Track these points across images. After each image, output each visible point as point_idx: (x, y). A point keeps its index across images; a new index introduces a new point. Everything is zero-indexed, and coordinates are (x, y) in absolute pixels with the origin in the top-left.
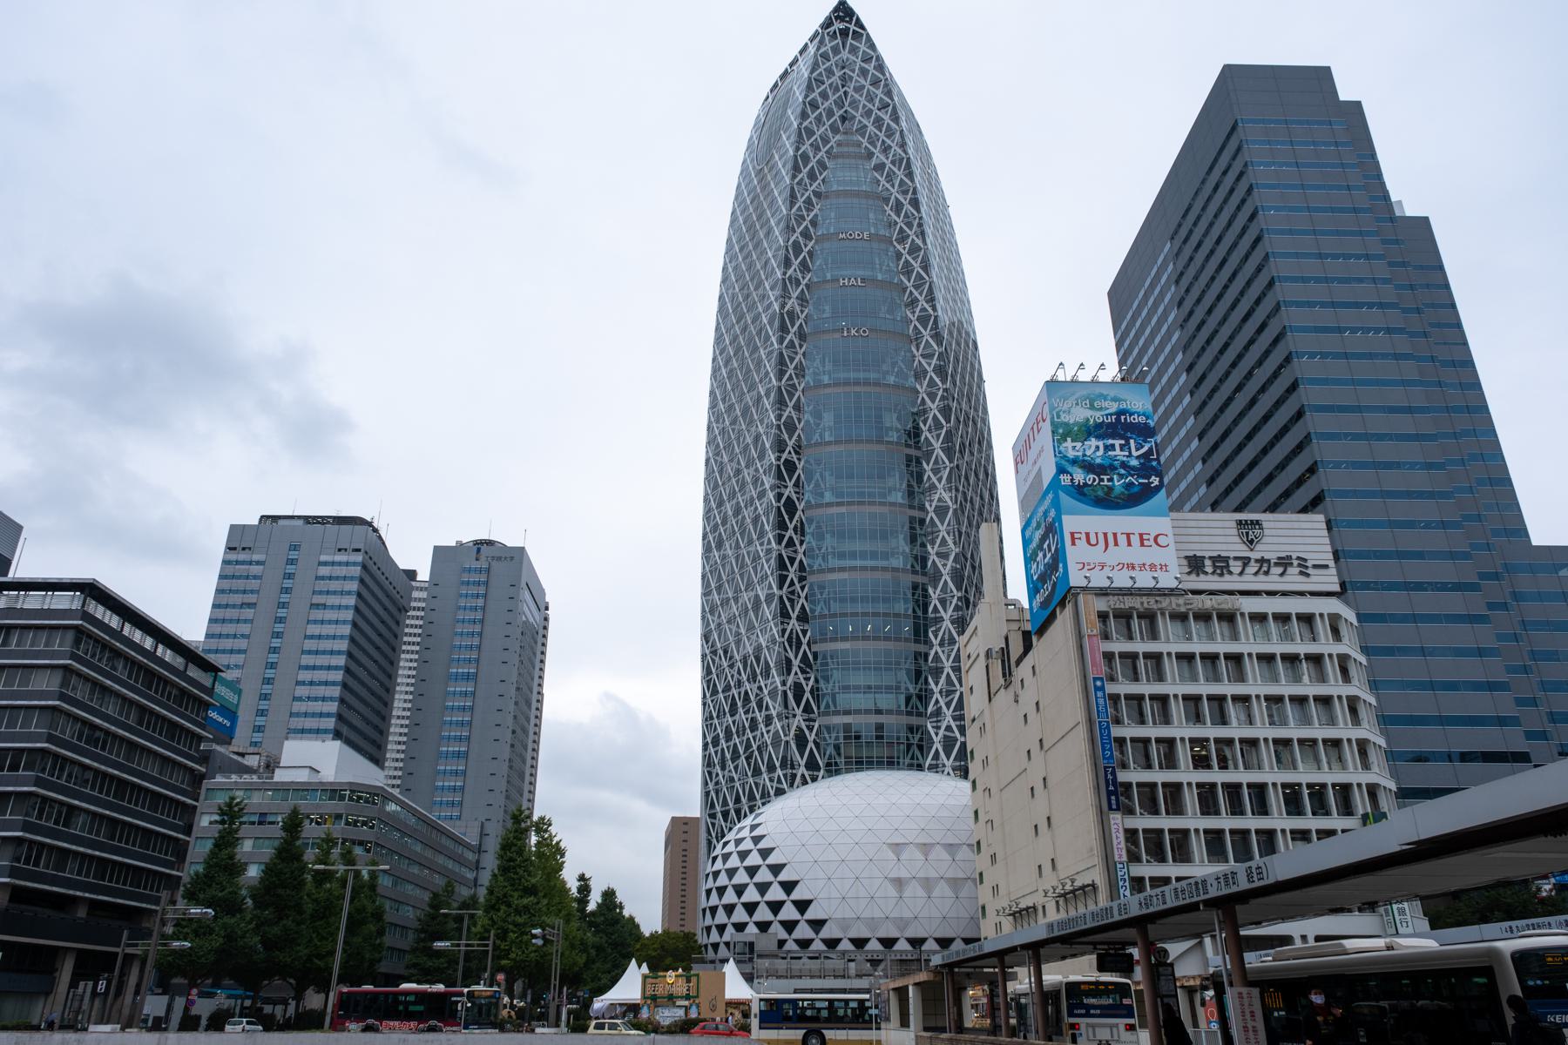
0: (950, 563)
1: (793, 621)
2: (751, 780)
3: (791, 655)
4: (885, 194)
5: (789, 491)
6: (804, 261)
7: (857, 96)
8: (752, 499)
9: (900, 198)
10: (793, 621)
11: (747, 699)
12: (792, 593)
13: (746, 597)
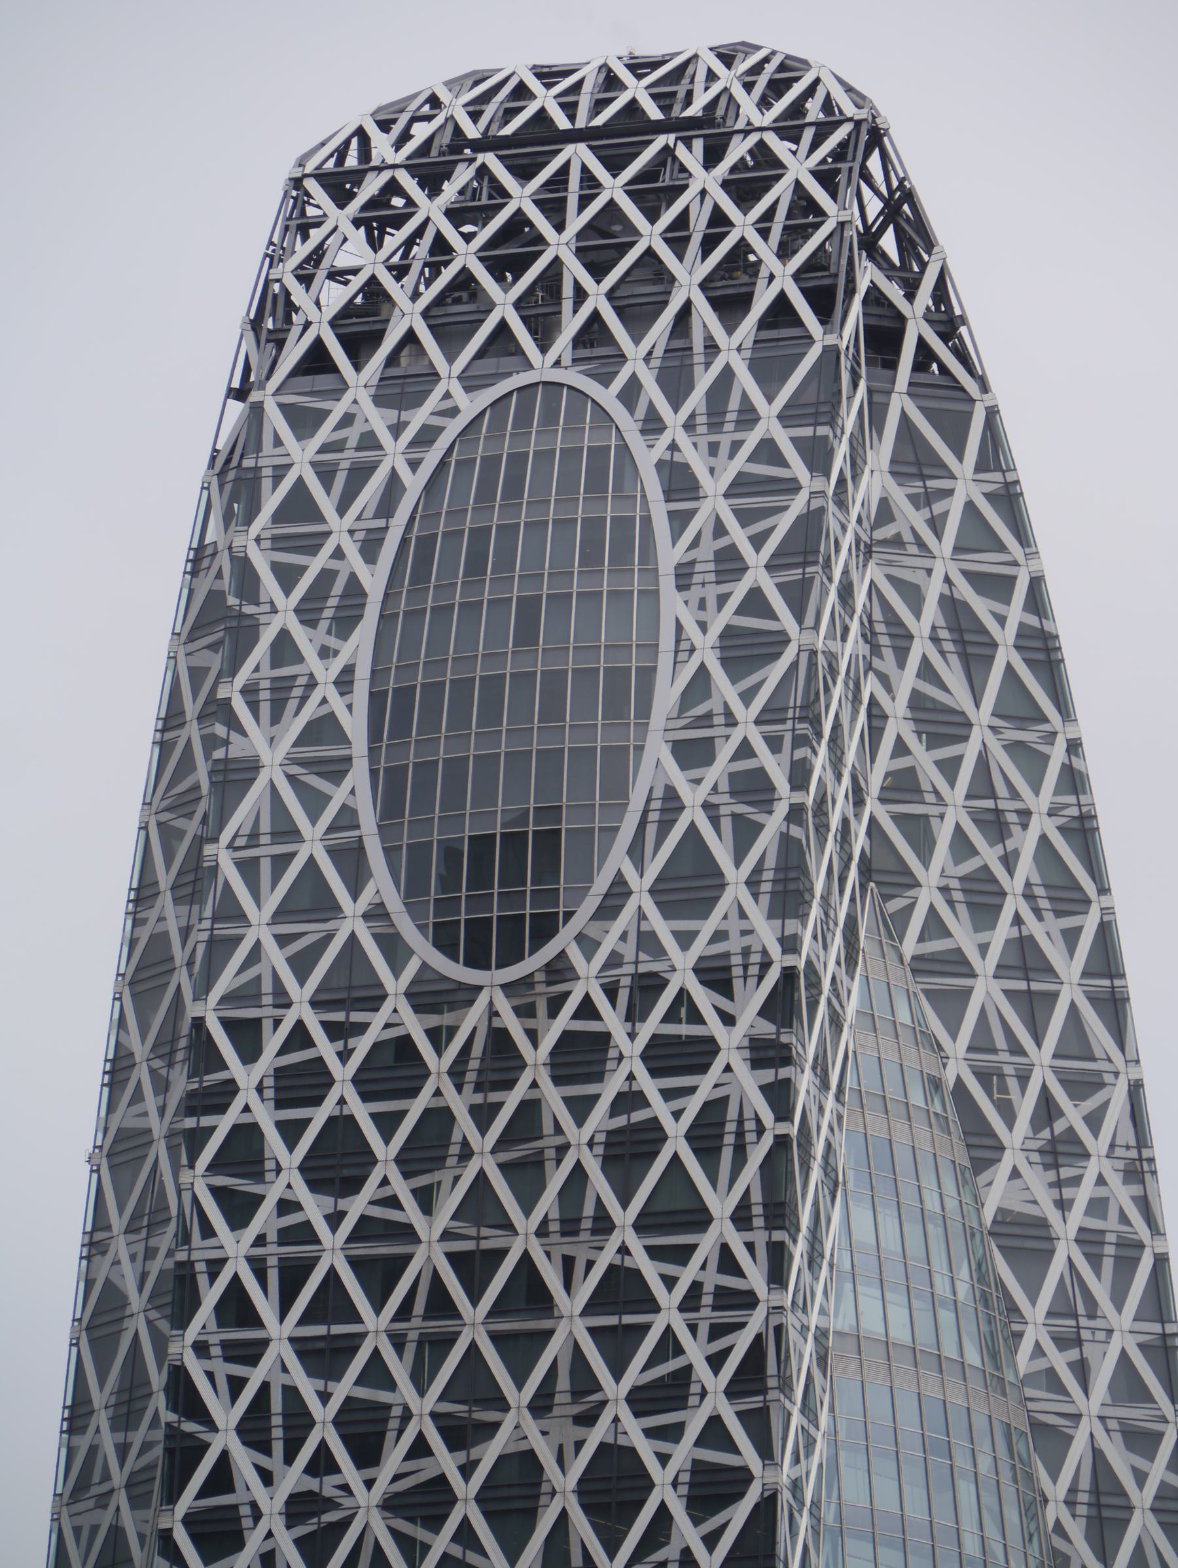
4: (1047, 1406)
7: (924, 759)
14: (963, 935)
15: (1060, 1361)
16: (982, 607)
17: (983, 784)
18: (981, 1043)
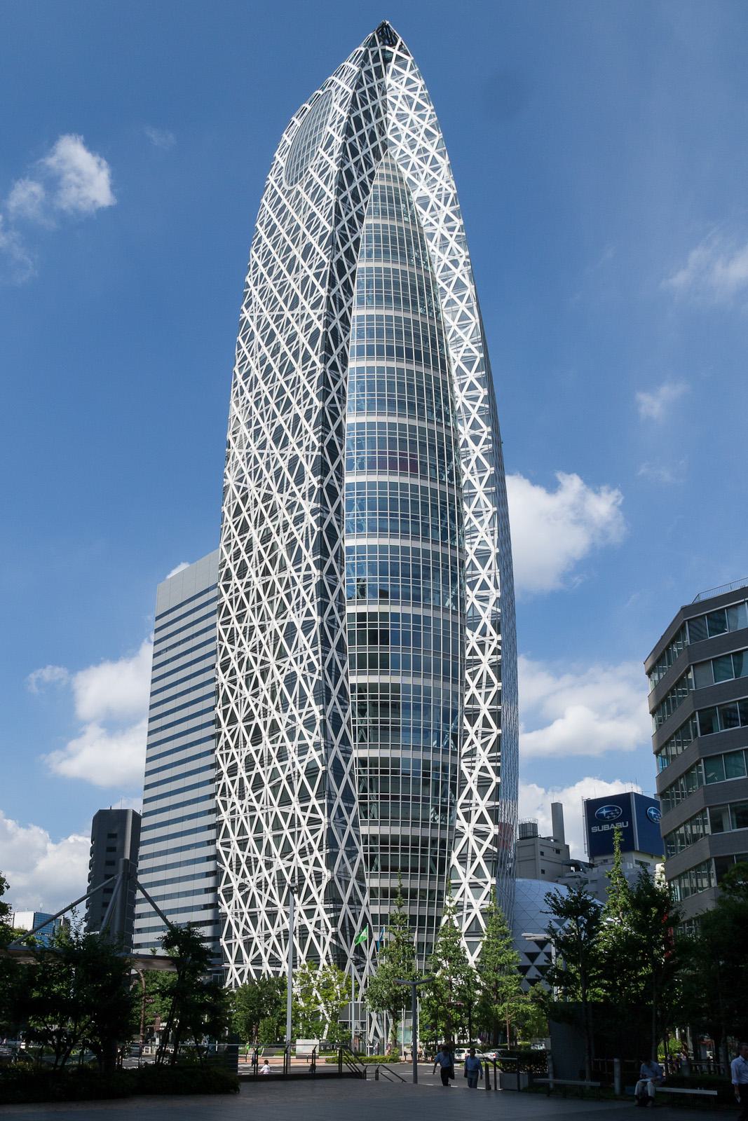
0: (490, 606)
1: (333, 651)
2: (277, 810)
3: (331, 687)
5: (331, 517)
6: (347, 282)
7: (399, 125)
8: (286, 525)
9: (447, 234)
10: (333, 651)
11: (274, 728)
12: (333, 621)
13: (274, 624)
14: (408, 151)
15: (432, 220)
16: (411, 94)
17: (412, 123)
18: (413, 168)
